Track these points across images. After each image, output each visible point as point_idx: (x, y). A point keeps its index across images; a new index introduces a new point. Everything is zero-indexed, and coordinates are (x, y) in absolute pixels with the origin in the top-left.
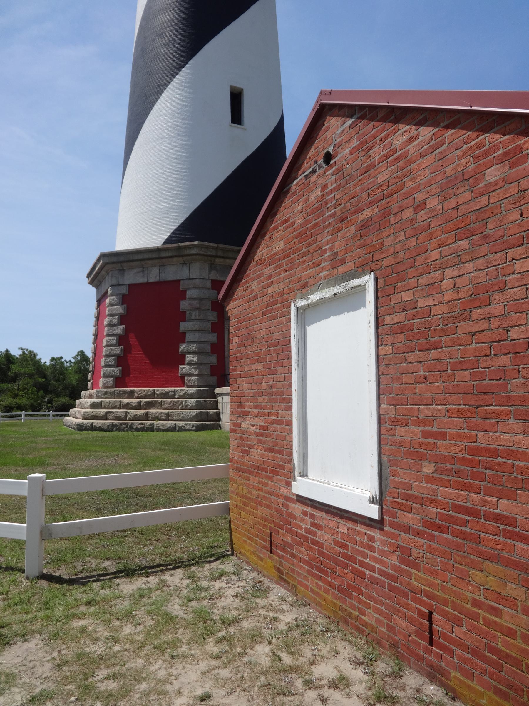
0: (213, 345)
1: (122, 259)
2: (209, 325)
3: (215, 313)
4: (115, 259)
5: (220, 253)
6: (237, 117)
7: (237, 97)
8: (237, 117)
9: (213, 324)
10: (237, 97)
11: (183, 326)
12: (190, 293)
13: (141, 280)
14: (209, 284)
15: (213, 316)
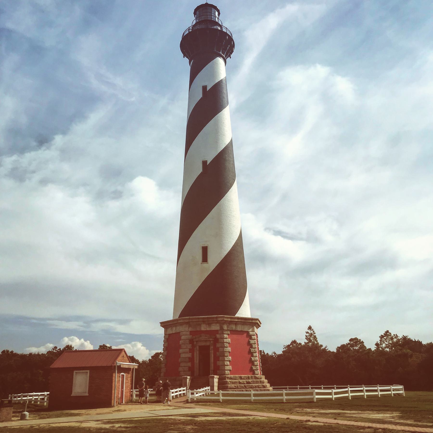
0: (189, 358)
1: (165, 325)
2: (187, 350)
3: (191, 345)
4: (163, 325)
5: (191, 321)
6: (205, 259)
7: (205, 250)
8: (205, 259)
9: (190, 349)
10: (205, 250)
11: (181, 351)
12: (183, 337)
13: (171, 332)
14: (188, 333)
15: (190, 346)
